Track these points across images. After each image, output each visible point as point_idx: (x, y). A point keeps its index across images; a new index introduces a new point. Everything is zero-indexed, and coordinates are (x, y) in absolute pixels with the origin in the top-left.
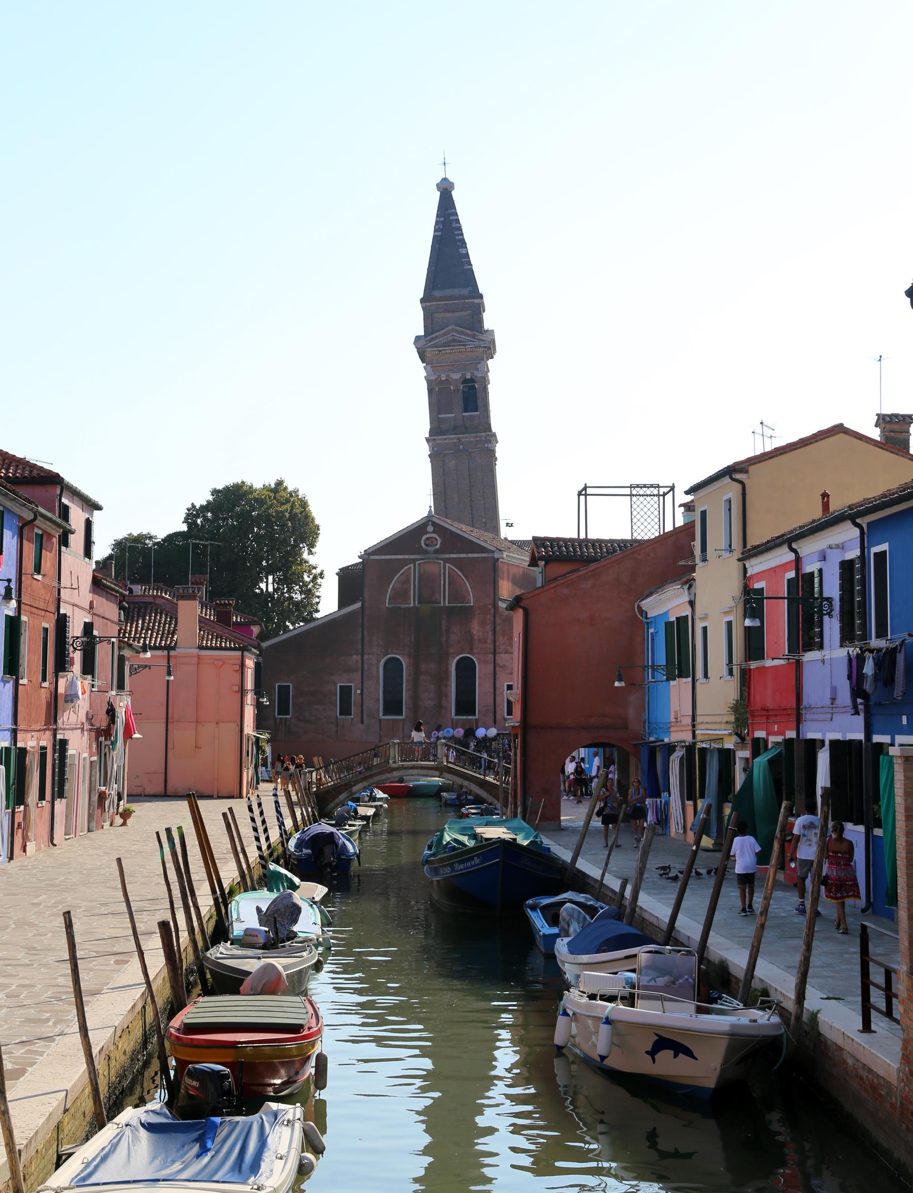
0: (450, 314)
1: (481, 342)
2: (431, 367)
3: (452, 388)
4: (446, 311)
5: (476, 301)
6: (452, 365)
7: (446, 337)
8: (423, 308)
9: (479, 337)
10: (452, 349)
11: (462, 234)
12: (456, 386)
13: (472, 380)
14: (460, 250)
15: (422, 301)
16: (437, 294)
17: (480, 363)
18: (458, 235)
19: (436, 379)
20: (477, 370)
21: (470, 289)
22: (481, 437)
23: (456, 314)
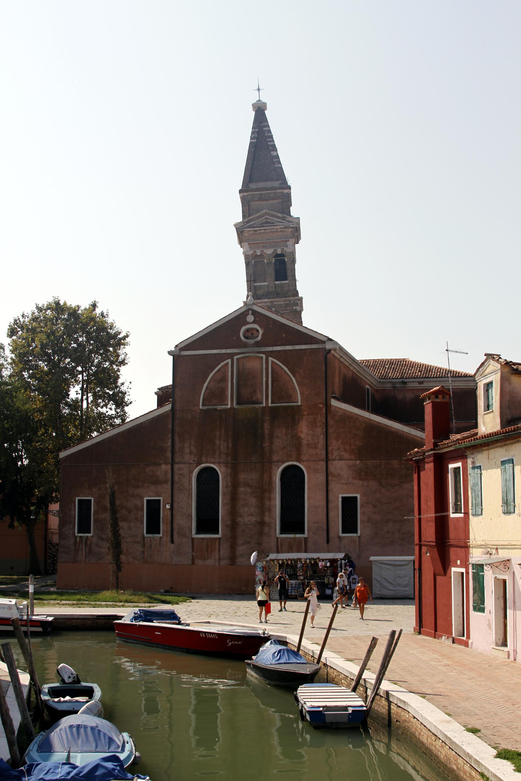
0: (265, 202)
1: (290, 223)
2: (249, 244)
3: (266, 261)
4: (260, 199)
5: (286, 191)
6: (266, 243)
7: (261, 219)
8: (243, 199)
9: (288, 219)
10: (266, 230)
11: (273, 141)
12: (269, 259)
13: (282, 255)
14: (272, 153)
15: (241, 191)
16: (253, 186)
17: (288, 241)
18: (270, 141)
19: (252, 254)
20: (287, 246)
21: (279, 182)
22: (290, 301)
23: (269, 202)
